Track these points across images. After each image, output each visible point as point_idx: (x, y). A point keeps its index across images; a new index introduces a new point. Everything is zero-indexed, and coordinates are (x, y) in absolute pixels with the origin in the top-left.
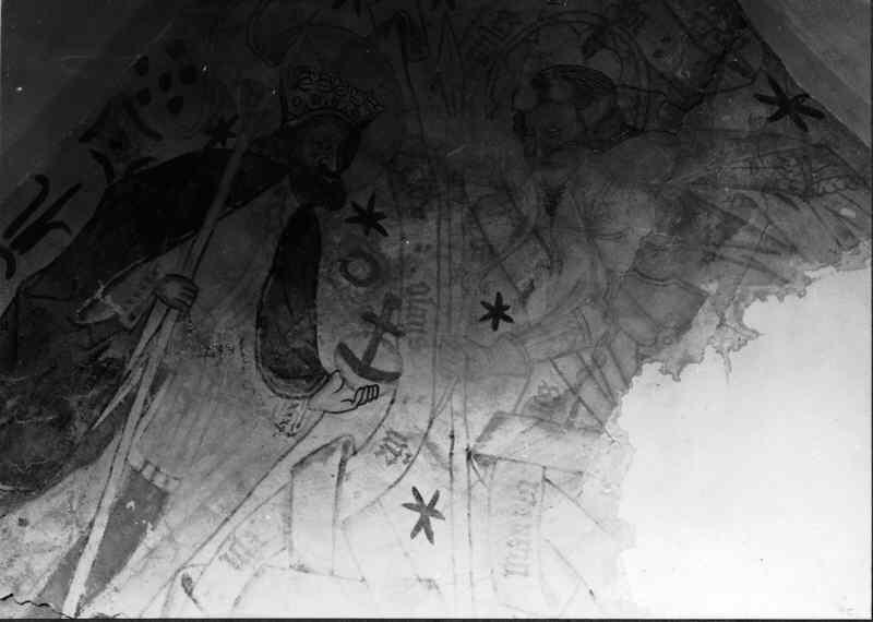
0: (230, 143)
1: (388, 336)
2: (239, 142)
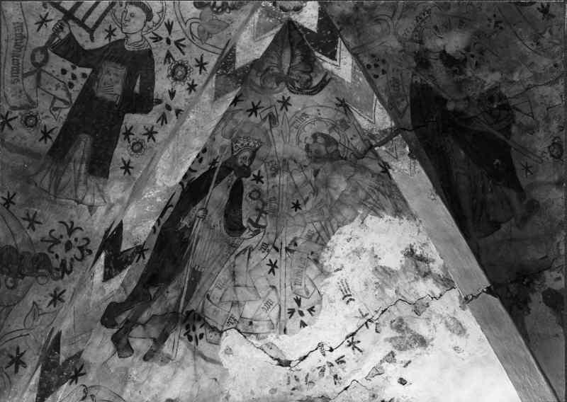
0: (216, 164)
1: (264, 215)
2: (219, 165)
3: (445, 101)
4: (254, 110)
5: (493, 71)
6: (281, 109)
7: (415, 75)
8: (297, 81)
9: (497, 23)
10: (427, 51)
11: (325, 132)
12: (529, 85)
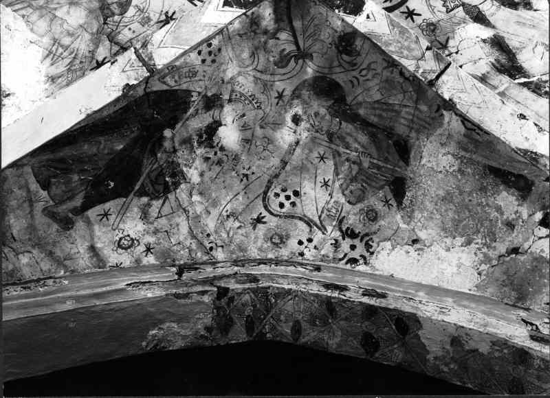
3: (172, 127)
5: (202, 175)
7: (199, 95)
9: (246, 176)
10: (222, 107)
12: (189, 212)
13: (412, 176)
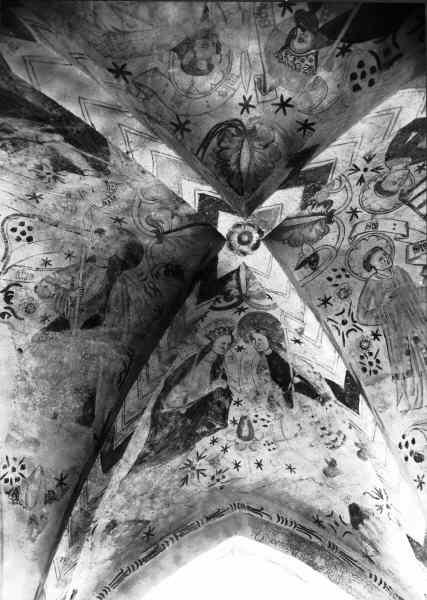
0: (341, 45)
2: (338, 44)
4: (284, 105)
6: (250, 98)
8: (233, 135)
11: (199, 79)
13: (74, 333)
